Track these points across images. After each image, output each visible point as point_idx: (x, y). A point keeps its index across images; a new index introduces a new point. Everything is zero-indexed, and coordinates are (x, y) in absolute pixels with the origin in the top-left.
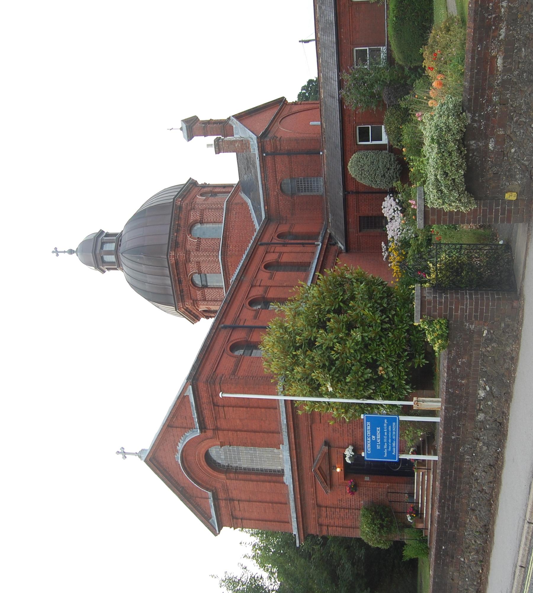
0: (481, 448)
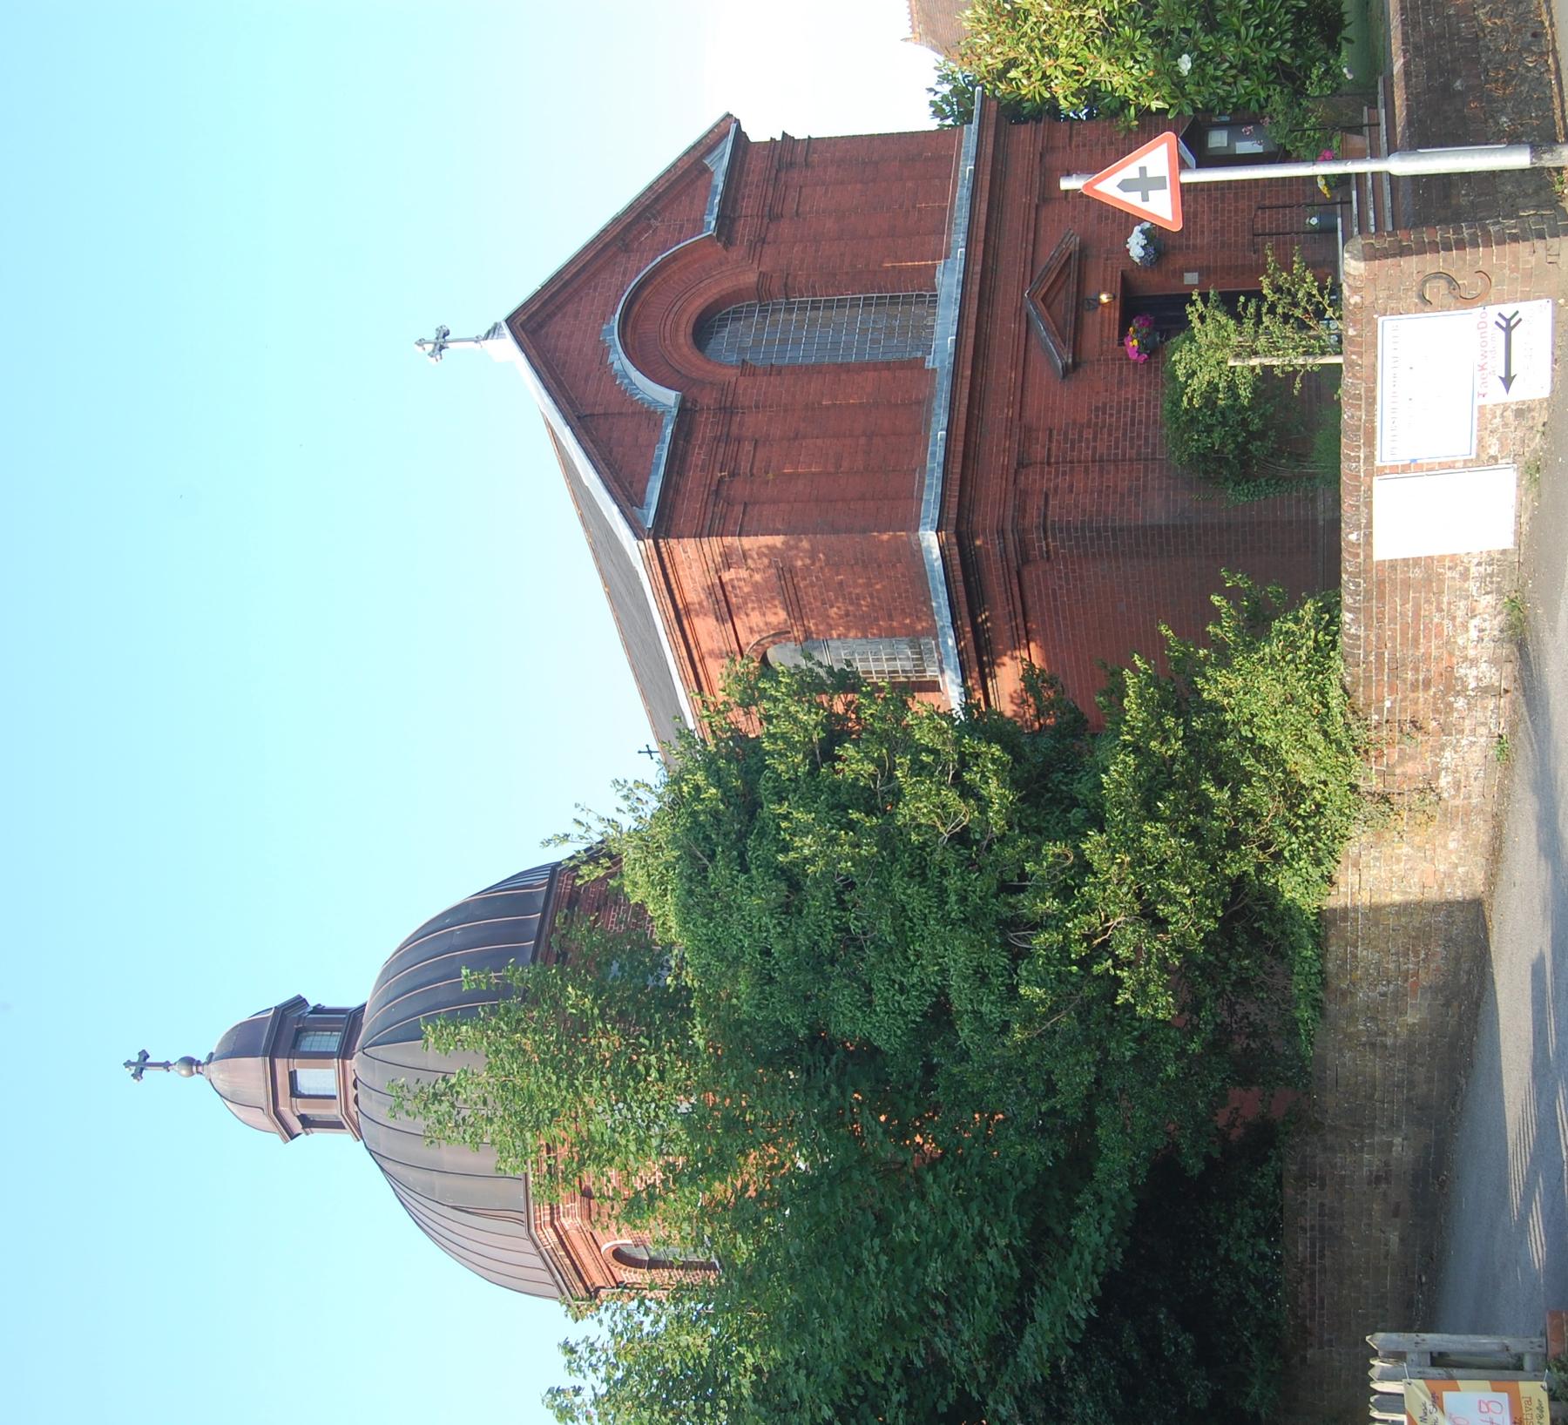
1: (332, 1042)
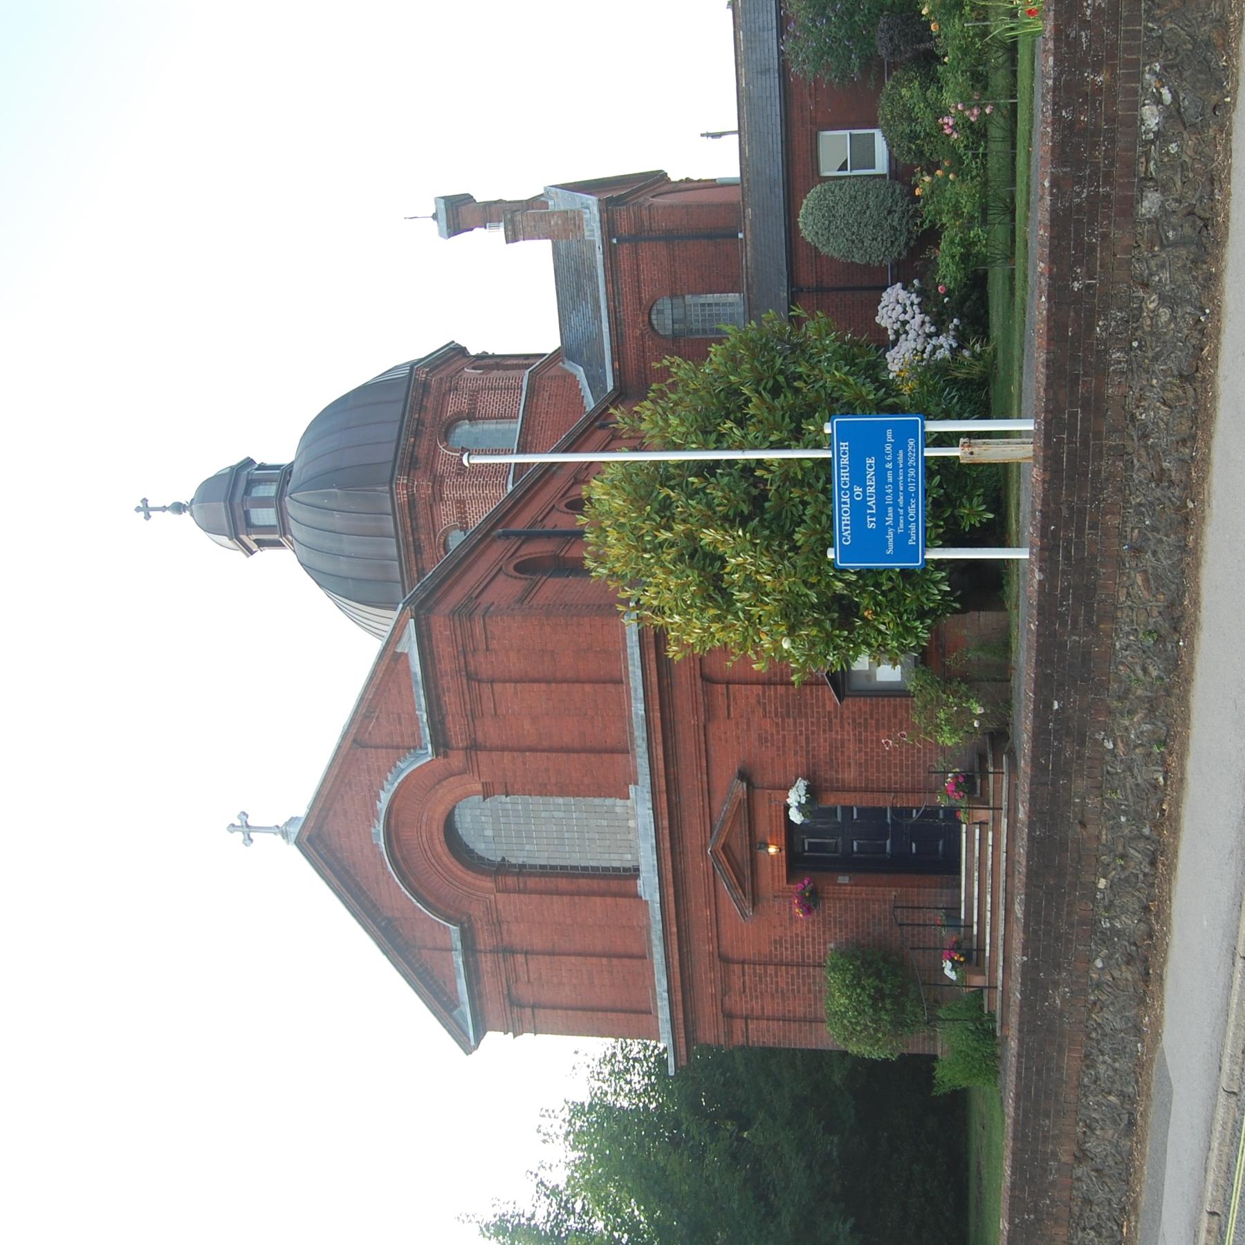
0: (1155, 315)
1: (270, 490)
